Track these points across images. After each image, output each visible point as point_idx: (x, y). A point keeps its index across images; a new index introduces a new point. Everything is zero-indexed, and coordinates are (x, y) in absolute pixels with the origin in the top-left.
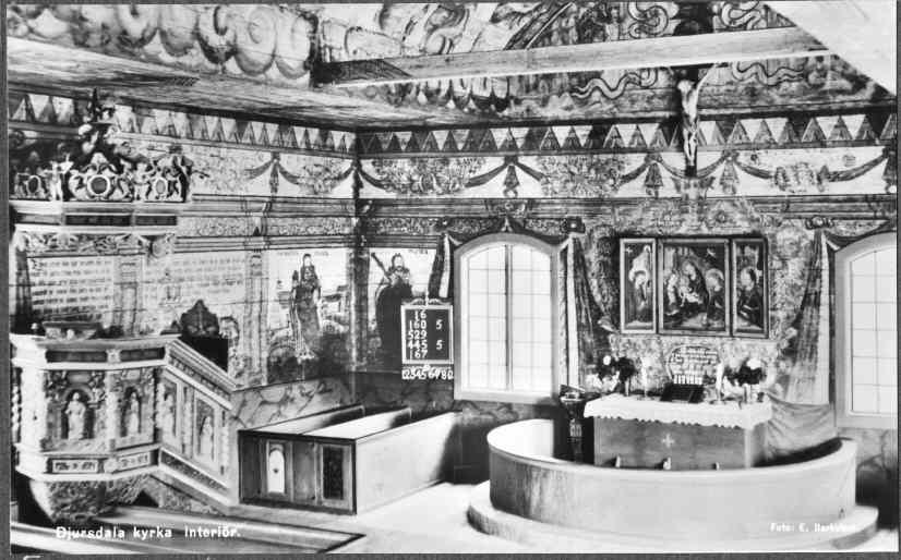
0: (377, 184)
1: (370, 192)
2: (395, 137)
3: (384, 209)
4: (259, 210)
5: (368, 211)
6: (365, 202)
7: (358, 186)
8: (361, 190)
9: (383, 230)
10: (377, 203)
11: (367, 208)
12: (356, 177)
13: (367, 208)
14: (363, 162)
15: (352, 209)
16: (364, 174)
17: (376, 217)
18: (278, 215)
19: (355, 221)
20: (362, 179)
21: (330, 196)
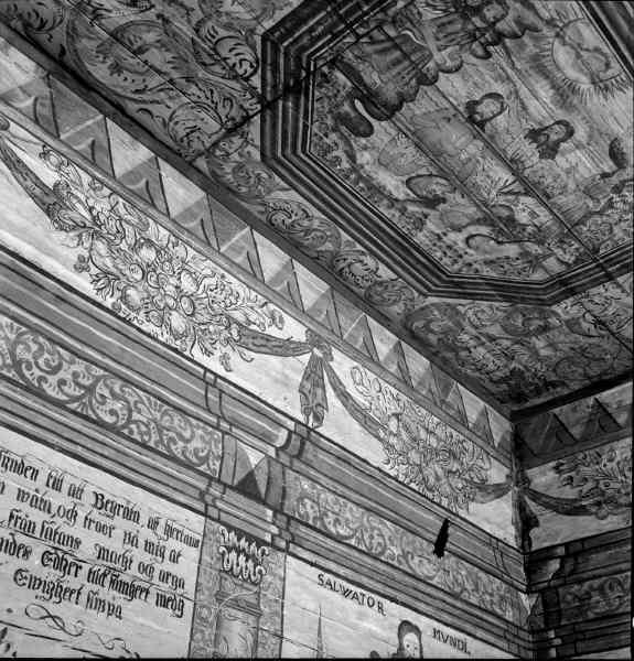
0: (573, 509)
1: (555, 530)
2: (599, 405)
3: (598, 558)
4: (266, 438)
5: (557, 575)
6: (547, 554)
7: (526, 523)
8: (534, 532)
9: (602, 608)
10: (577, 551)
11: (555, 565)
12: (521, 507)
13: (555, 565)
14: (529, 472)
15: (519, 573)
16: (536, 496)
17: (580, 582)
18: (324, 480)
19: (527, 601)
20: (533, 506)
21: (462, 513)
